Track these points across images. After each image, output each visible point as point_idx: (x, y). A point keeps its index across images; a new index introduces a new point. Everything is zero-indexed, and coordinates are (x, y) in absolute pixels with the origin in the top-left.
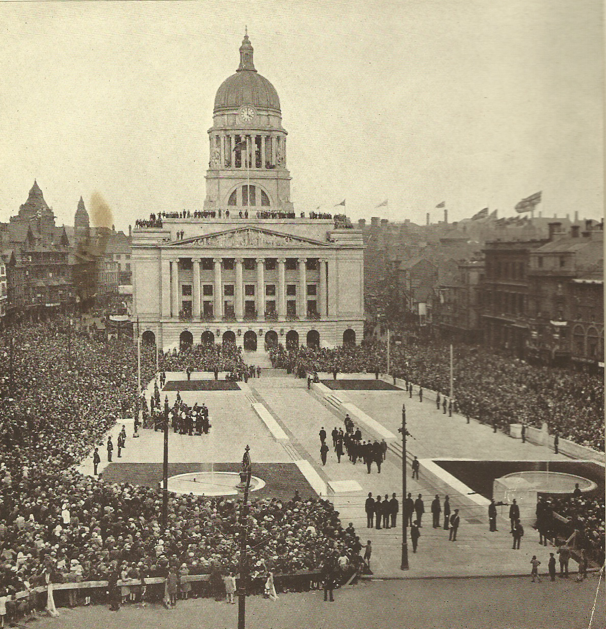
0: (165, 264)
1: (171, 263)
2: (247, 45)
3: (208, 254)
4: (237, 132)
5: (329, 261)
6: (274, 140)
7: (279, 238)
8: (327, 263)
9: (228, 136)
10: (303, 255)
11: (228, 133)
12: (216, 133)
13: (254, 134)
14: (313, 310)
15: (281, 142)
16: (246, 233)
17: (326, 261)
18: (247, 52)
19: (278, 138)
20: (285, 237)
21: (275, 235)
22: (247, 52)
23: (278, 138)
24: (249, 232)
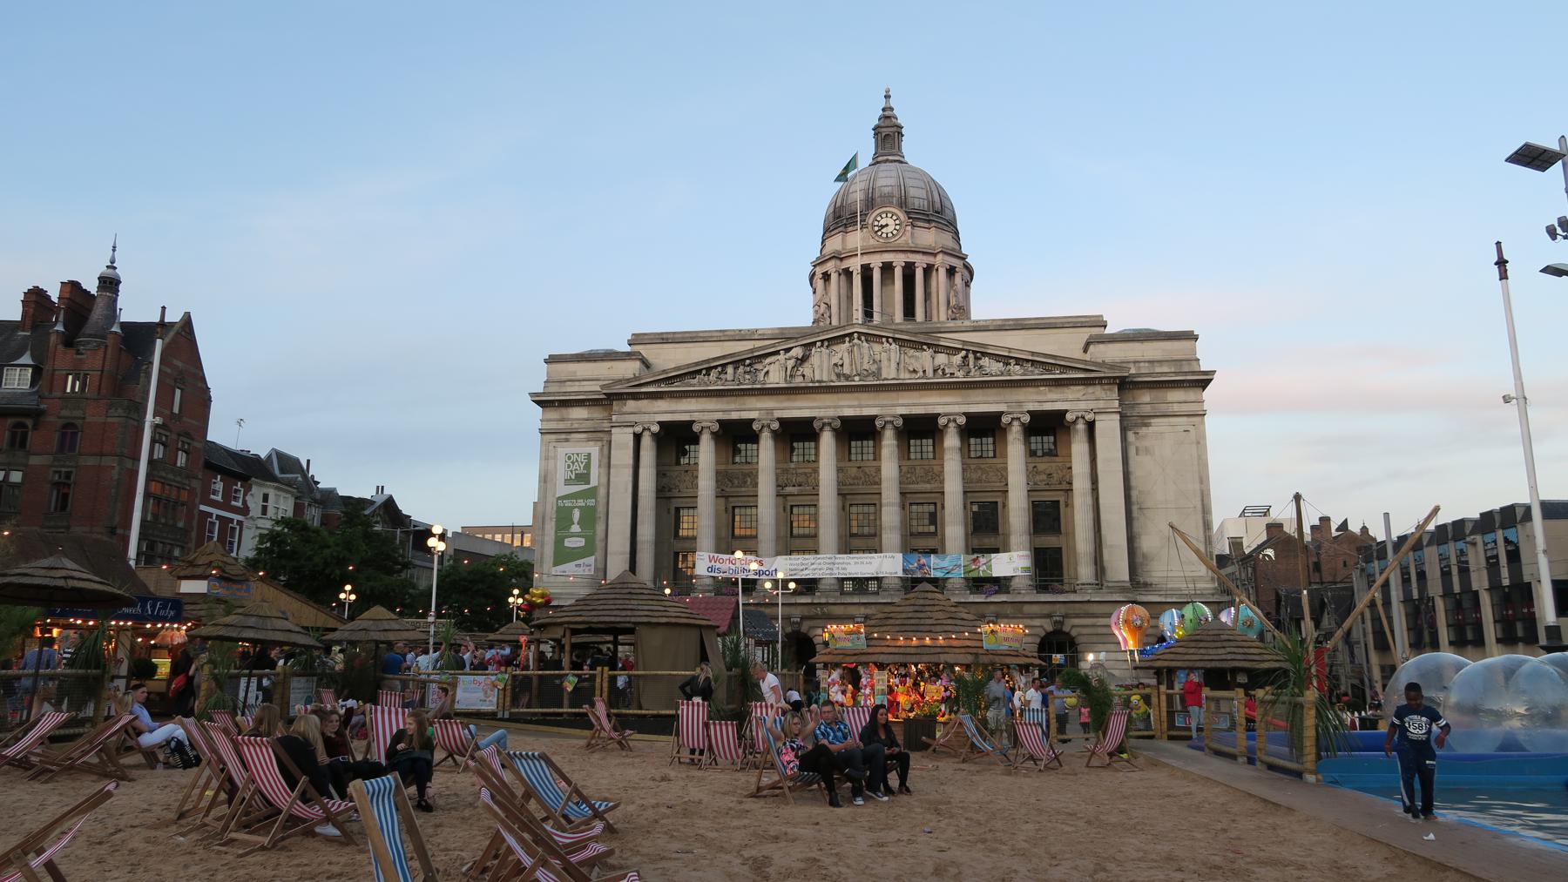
0: (622, 438)
1: (637, 438)
2: (887, 122)
3: (737, 410)
4: (866, 260)
6: (942, 273)
7: (941, 359)
8: (1091, 426)
9: (848, 273)
11: (845, 265)
12: (819, 271)
13: (899, 260)
15: (958, 279)
16: (847, 344)
17: (1089, 417)
18: (888, 135)
21: (929, 346)
22: (888, 135)
23: (951, 272)
24: (856, 341)
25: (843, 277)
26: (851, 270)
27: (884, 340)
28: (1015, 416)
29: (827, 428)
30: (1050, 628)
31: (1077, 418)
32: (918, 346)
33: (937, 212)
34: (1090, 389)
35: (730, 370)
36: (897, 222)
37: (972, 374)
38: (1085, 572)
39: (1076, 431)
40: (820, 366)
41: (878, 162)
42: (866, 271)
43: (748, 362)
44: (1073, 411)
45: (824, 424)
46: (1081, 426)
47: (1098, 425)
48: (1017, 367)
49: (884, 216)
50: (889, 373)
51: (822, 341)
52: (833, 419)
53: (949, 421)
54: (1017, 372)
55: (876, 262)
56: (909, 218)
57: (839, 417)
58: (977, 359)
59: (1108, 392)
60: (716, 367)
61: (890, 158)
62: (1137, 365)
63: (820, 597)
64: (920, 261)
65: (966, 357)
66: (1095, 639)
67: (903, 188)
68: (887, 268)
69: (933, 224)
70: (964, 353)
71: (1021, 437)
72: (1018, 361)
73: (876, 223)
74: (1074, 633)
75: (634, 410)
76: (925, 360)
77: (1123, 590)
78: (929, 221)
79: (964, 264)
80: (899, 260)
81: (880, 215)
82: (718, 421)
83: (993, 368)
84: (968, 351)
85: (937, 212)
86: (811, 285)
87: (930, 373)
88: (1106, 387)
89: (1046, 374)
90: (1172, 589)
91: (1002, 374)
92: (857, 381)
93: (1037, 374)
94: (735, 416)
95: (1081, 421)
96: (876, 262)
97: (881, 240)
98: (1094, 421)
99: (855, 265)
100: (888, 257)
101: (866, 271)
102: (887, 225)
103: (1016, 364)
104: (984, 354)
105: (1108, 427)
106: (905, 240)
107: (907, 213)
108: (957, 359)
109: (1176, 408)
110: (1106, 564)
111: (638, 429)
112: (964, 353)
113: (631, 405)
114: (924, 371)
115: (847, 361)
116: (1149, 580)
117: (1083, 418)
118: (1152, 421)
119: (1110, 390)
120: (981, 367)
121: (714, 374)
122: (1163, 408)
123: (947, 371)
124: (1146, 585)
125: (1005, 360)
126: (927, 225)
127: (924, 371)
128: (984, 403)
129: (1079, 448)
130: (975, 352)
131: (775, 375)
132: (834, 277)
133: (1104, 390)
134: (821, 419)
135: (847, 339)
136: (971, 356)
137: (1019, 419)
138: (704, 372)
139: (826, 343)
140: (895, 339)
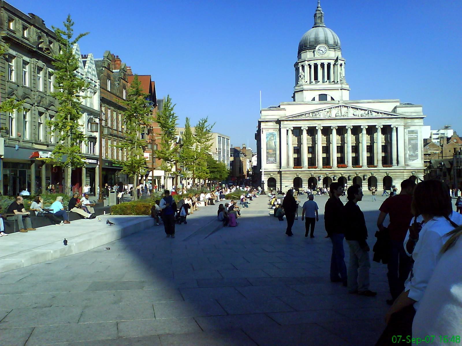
1: (287, 131)
4: (315, 62)
5: (398, 127)
6: (339, 66)
7: (363, 112)
8: (397, 128)
9: (309, 65)
10: (379, 124)
14: (387, 161)
15: (343, 66)
16: (339, 108)
17: (397, 127)
19: (341, 65)
20: (367, 110)
24: (342, 107)
25: (308, 66)
26: (311, 65)
27: (349, 107)
28: (379, 126)
29: (334, 129)
30: (386, 175)
31: (394, 127)
32: (357, 109)
33: (336, 45)
35: (311, 114)
36: (325, 50)
37: (370, 116)
38: (395, 162)
39: (393, 130)
40: (334, 113)
41: (316, 27)
42: (316, 66)
43: (315, 112)
45: (334, 128)
46: (395, 129)
49: (321, 47)
50: (351, 116)
51: (333, 107)
52: (336, 126)
53: (364, 127)
54: (380, 116)
55: (319, 63)
56: (329, 48)
57: (337, 126)
58: (371, 112)
60: (307, 114)
61: (321, 25)
63: (333, 169)
64: (332, 62)
65: (368, 112)
66: (395, 177)
68: (322, 65)
69: (336, 50)
70: (368, 111)
71: (381, 131)
72: (381, 113)
74: (391, 176)
75: (286, 124)
76: (359, 113)
77: (402, 167)
78: (334, 49)
80: (326, 62)
82: (308, 127)
83: (374, 114)
84: (369, 110)
86: (295, 67)
87: (360, 116)
90: (413, 166)
91: (377, 116)
92: (342, 117)
93: (385, 116)
94: (312, 126)
96: (319, 63)
97: (320, 55)
99: (312, 63)
100: (322, 61)
101: (316, 66)
104: (373, 111)
105: (401, 130)
106: (326, 55)
107: (328, 46)
108: (366, 112)
109: (417, 124)
110: (399, 161)
111: (288, 129)
112: (368, 111)
113: (286, 122)
114: (358, 115)
115: (340, 112)
116: (408, 164)
117: (395, 126)
120: (372, 114)
121: (307, 115)
122: (413, 124)
123: (364, 115)
124: (408, 165)
125: (378, 113)
126: (334, 50)
127: (358, 115)
128: (372, 123)
129: (394, 134)
130: (370, 111)
131: (322, 115)
132: (305, 67)
134: (333, 126)
135: (340, 107)
136: (370, 112)
137: (380, 127)
138: (304, 115)
139: (334, 108)
140: (351, 107)
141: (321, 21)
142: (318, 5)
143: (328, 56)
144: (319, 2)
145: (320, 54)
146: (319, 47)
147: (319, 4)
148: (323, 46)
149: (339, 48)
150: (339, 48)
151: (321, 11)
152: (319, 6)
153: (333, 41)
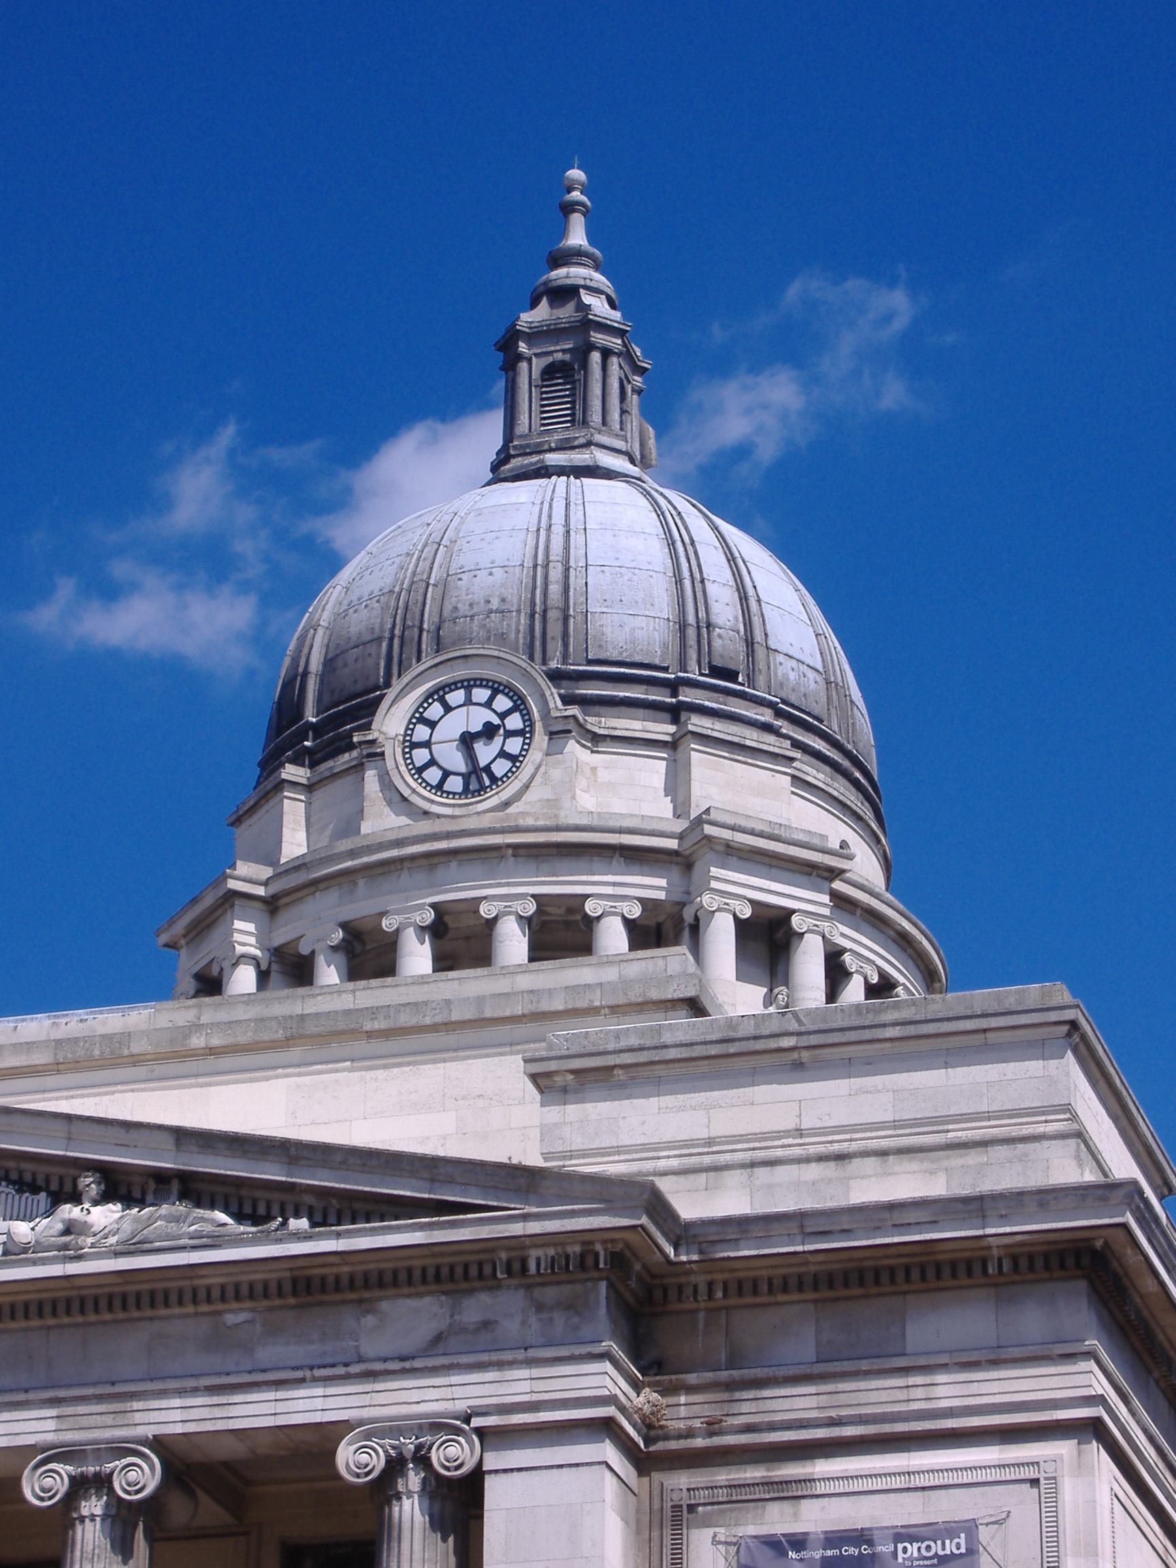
31: (395, 1466)
33: (731, 675)
34: (475, 1308)
44: (374, 1430)
47: (496, 1493)
48: (104, 1216)
49: (455, 697)
59: (559, 1319)
62: (761, 1172)
67: (556, 573)
69: (697, 723)
73: (514, 745)
78: (675, 713)
79: (836, 896)
81: (438, 694)
85: (731, 675)
88: (550, 1294)
89: (237, 1241)
95: (413, 1479)
98: (476, 1479)
102: (467, 741)
103: (105, 1198)
117: (422, 1459)
118: (822, 1467)
119: (570, 1306)
126: (663, 730)
133: (540, 1308)
141: (579, 419)
142: (564, 232)
143: (553, 803)
144: (576, 195)
145: (439, 787)
146: (429, 696)
147: (577, 223)
148: (481, 682)
149: (766, 716)
150: (766, 716)
151: (587, 299)
152: (577, 237)
153: (664, 606)
